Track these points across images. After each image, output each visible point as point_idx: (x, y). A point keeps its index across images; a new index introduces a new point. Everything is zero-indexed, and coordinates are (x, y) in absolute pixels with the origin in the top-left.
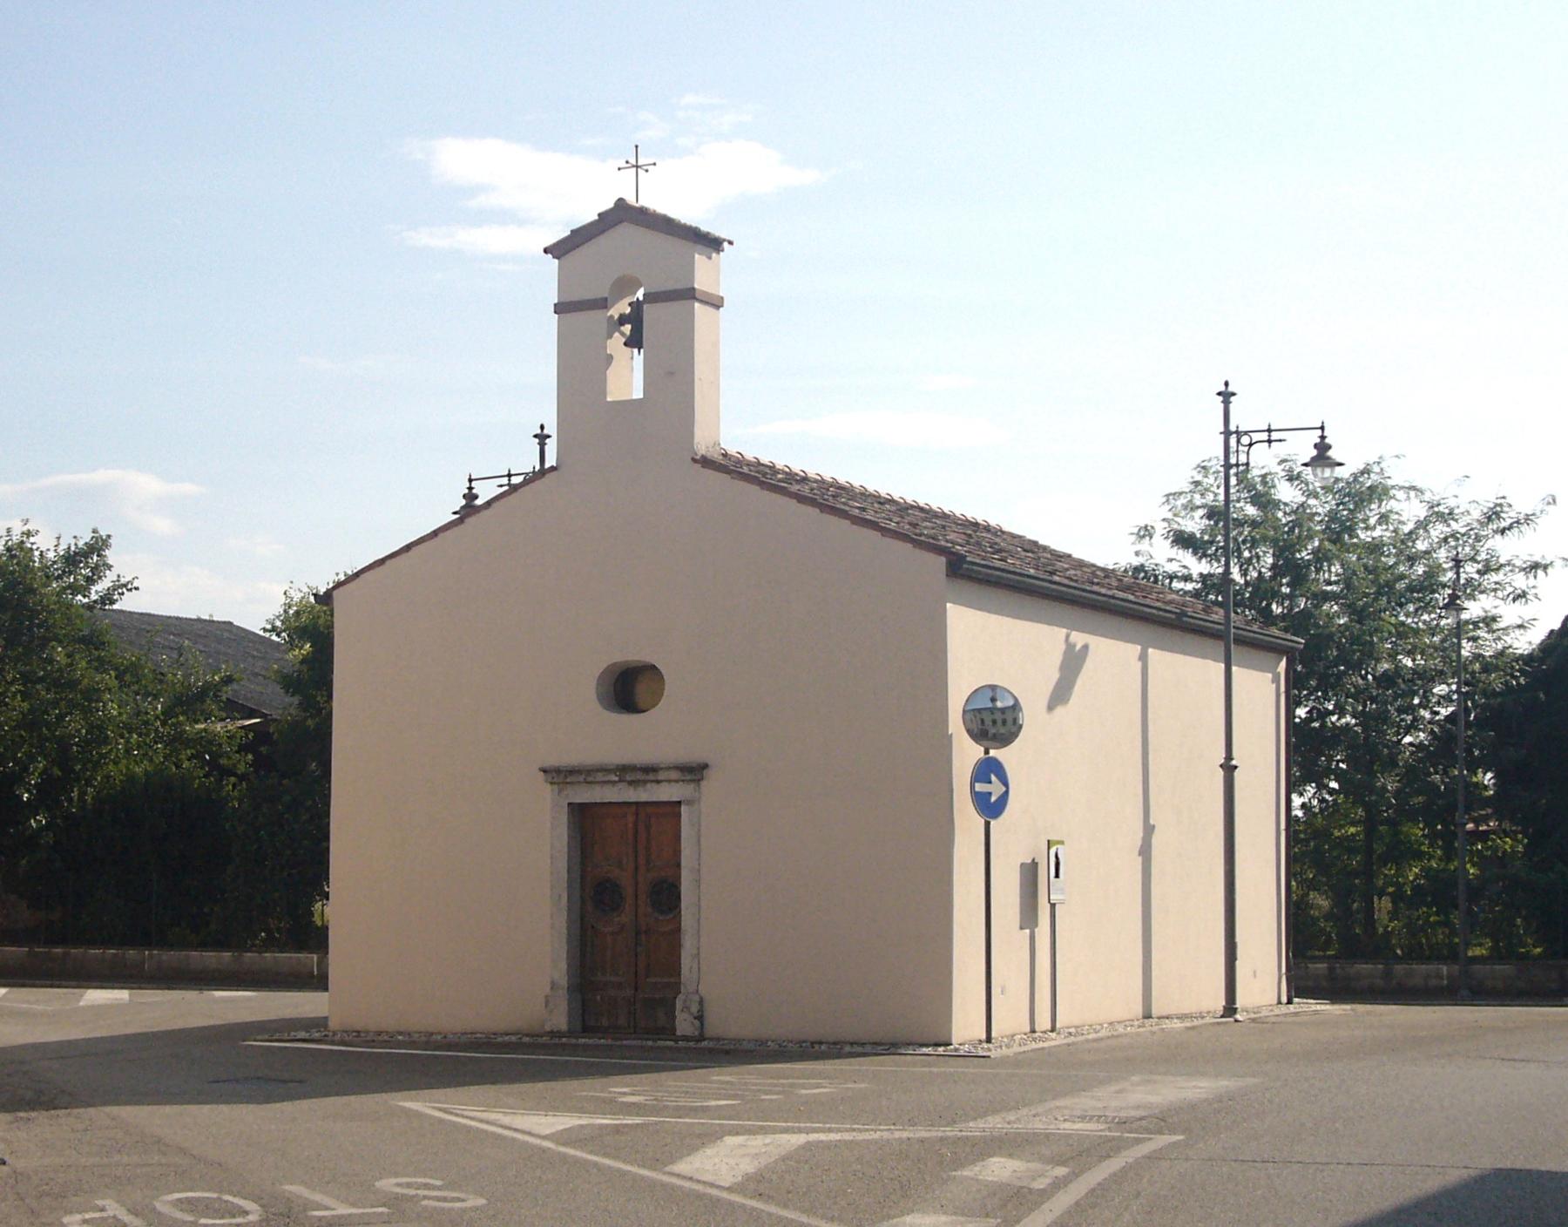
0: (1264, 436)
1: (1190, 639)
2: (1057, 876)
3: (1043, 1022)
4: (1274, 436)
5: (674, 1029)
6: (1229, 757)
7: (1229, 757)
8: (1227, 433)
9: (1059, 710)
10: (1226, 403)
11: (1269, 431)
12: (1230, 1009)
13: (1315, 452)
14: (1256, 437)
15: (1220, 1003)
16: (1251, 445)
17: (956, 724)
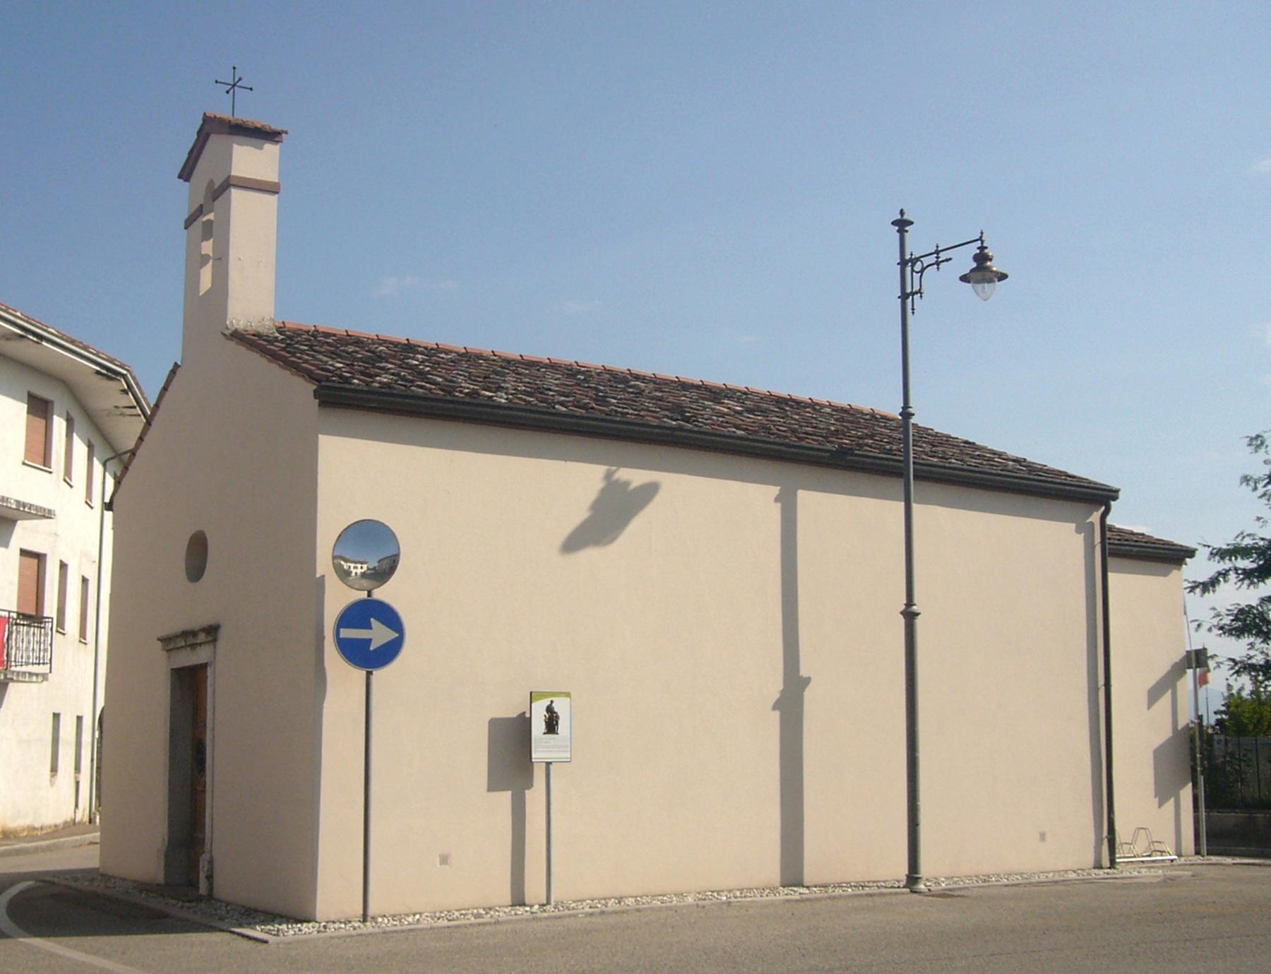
0: (932, 259)
1: (863, 479)
2: (79, 719)
3: (534, 888)
4: (943, 256)
5: (802, 879)
6: (910, 602)
7: (910, 602)
8: (903, 263)
9: (590, 555)
10: (902, 232)
11: (937, 252)
12: (913, 878)
13: (975, 265)
14: (926, 261)
15: (903, 870)
16: (922, 271)
17: (324, 564)
